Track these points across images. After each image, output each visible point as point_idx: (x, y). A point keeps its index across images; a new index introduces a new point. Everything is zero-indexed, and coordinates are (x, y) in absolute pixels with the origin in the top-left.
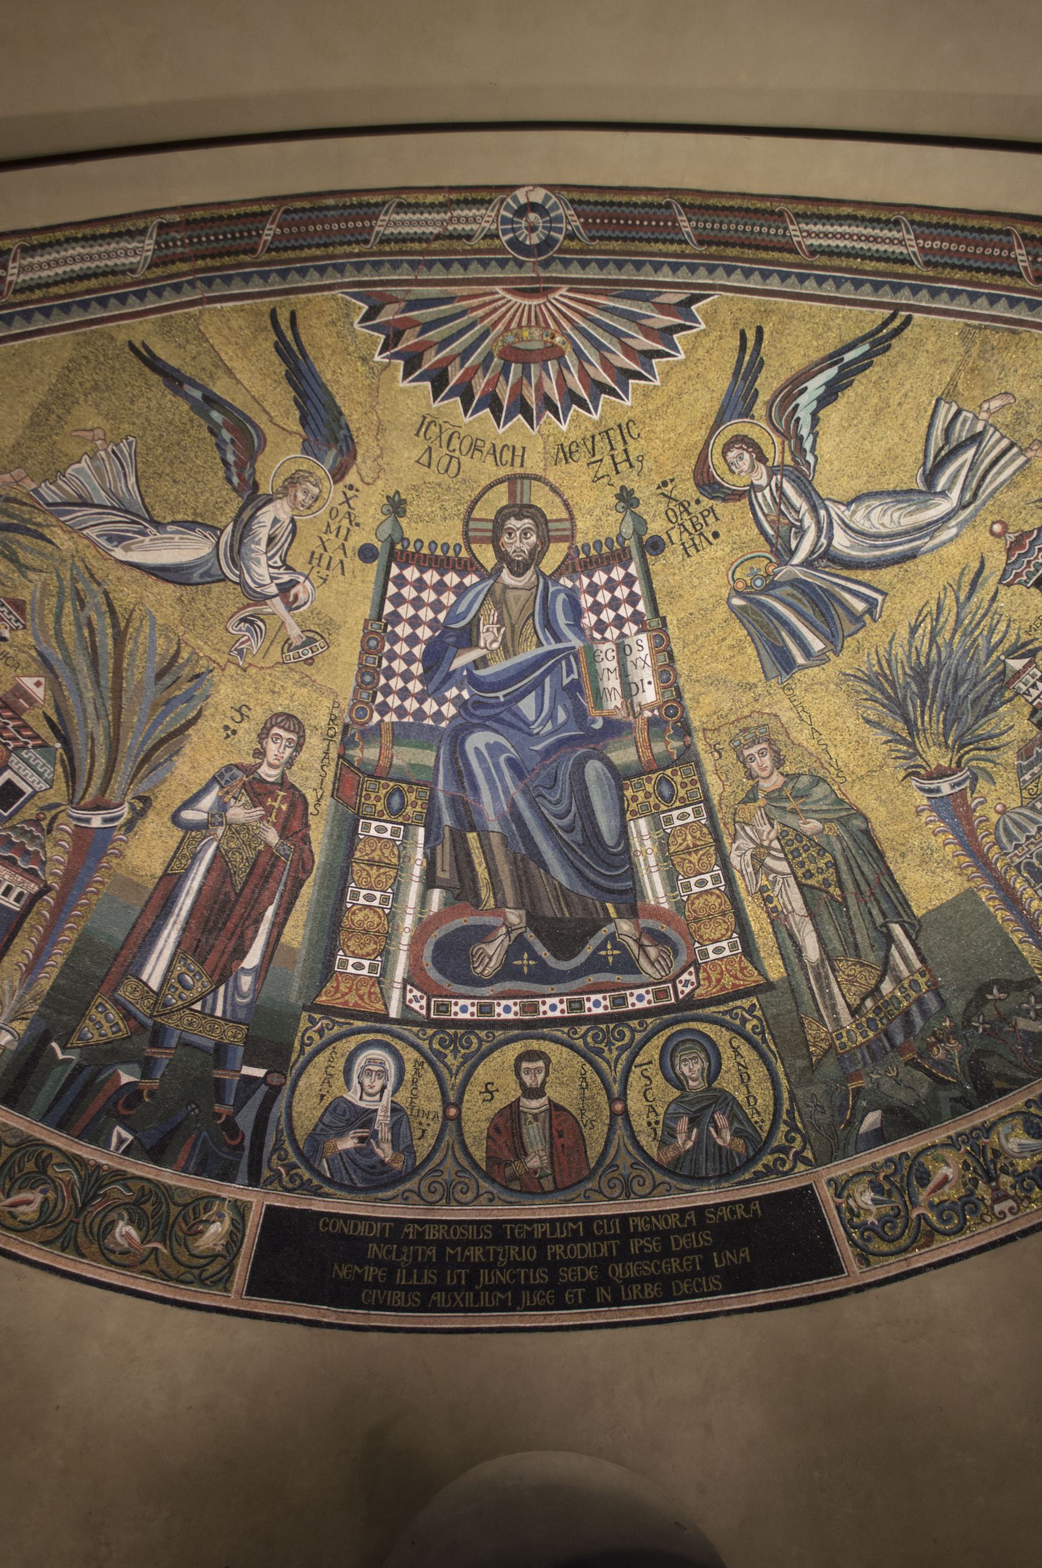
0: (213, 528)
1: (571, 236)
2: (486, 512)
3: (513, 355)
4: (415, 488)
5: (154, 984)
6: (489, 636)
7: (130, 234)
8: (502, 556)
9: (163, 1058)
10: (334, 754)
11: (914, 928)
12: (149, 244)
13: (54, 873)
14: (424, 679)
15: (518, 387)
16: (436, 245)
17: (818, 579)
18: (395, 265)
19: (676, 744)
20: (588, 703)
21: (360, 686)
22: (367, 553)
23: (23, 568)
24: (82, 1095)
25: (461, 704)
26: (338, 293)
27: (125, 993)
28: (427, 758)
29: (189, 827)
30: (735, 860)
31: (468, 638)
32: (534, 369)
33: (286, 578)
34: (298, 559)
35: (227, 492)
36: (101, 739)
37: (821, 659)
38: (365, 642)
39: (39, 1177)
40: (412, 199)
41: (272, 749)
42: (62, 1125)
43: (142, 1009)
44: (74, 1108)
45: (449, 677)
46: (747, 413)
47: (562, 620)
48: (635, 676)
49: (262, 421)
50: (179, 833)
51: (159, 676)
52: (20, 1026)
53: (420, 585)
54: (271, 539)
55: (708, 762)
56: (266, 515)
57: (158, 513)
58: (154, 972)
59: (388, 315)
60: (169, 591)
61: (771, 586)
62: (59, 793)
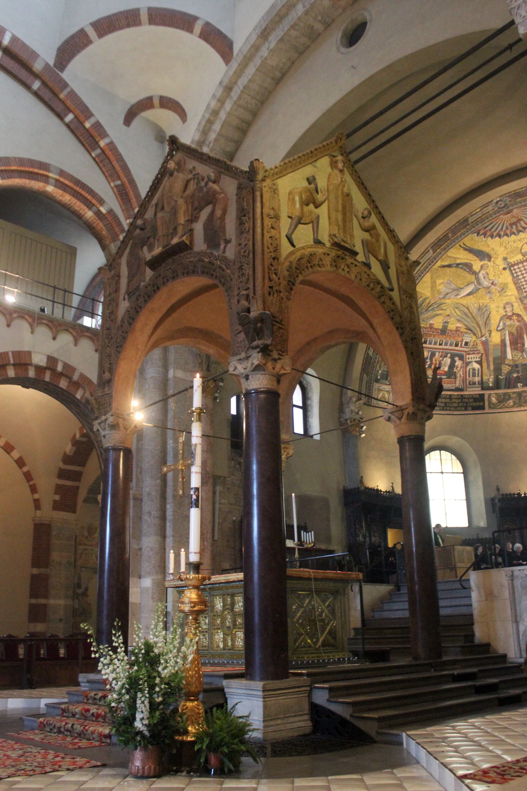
0: (472, 283)
1: (510, 201)
3: (511, 225)
4: (507, 254)
5: (511, 358)
7: (427, 252)
9: (520, 369)
10: (520, 304)
12: (431, 251)
13: (482, 351)
15: (517, 229)
16: (483, 217)
18: (478, 224)
21: (518, 291)
22: (504, 269)
23: (445, 310)
24: (509, 381)
26: (470, 235)
27: (507, 362)
29: (500, 330)
32: (518, 224)
33: (491, 282)
34: (491, 277)
35: (471, 276)
36: (475, 325)
38: (514, 282)
39: (510, 398)
40: (473, 213)
41: (508, 309)
42: (509, 388)
43: (511, 363)
44: (509, 384)
49: (469, 261)
50: (499, 332)
51: (479, 310)
52: (492, 377)
53: (519, 268)
54: (484, 278)
56: (481, 275)
57: (461, 286)
58: (509, 356)
59: (481, 233)
60: (471, 297)
62: (474, 338)
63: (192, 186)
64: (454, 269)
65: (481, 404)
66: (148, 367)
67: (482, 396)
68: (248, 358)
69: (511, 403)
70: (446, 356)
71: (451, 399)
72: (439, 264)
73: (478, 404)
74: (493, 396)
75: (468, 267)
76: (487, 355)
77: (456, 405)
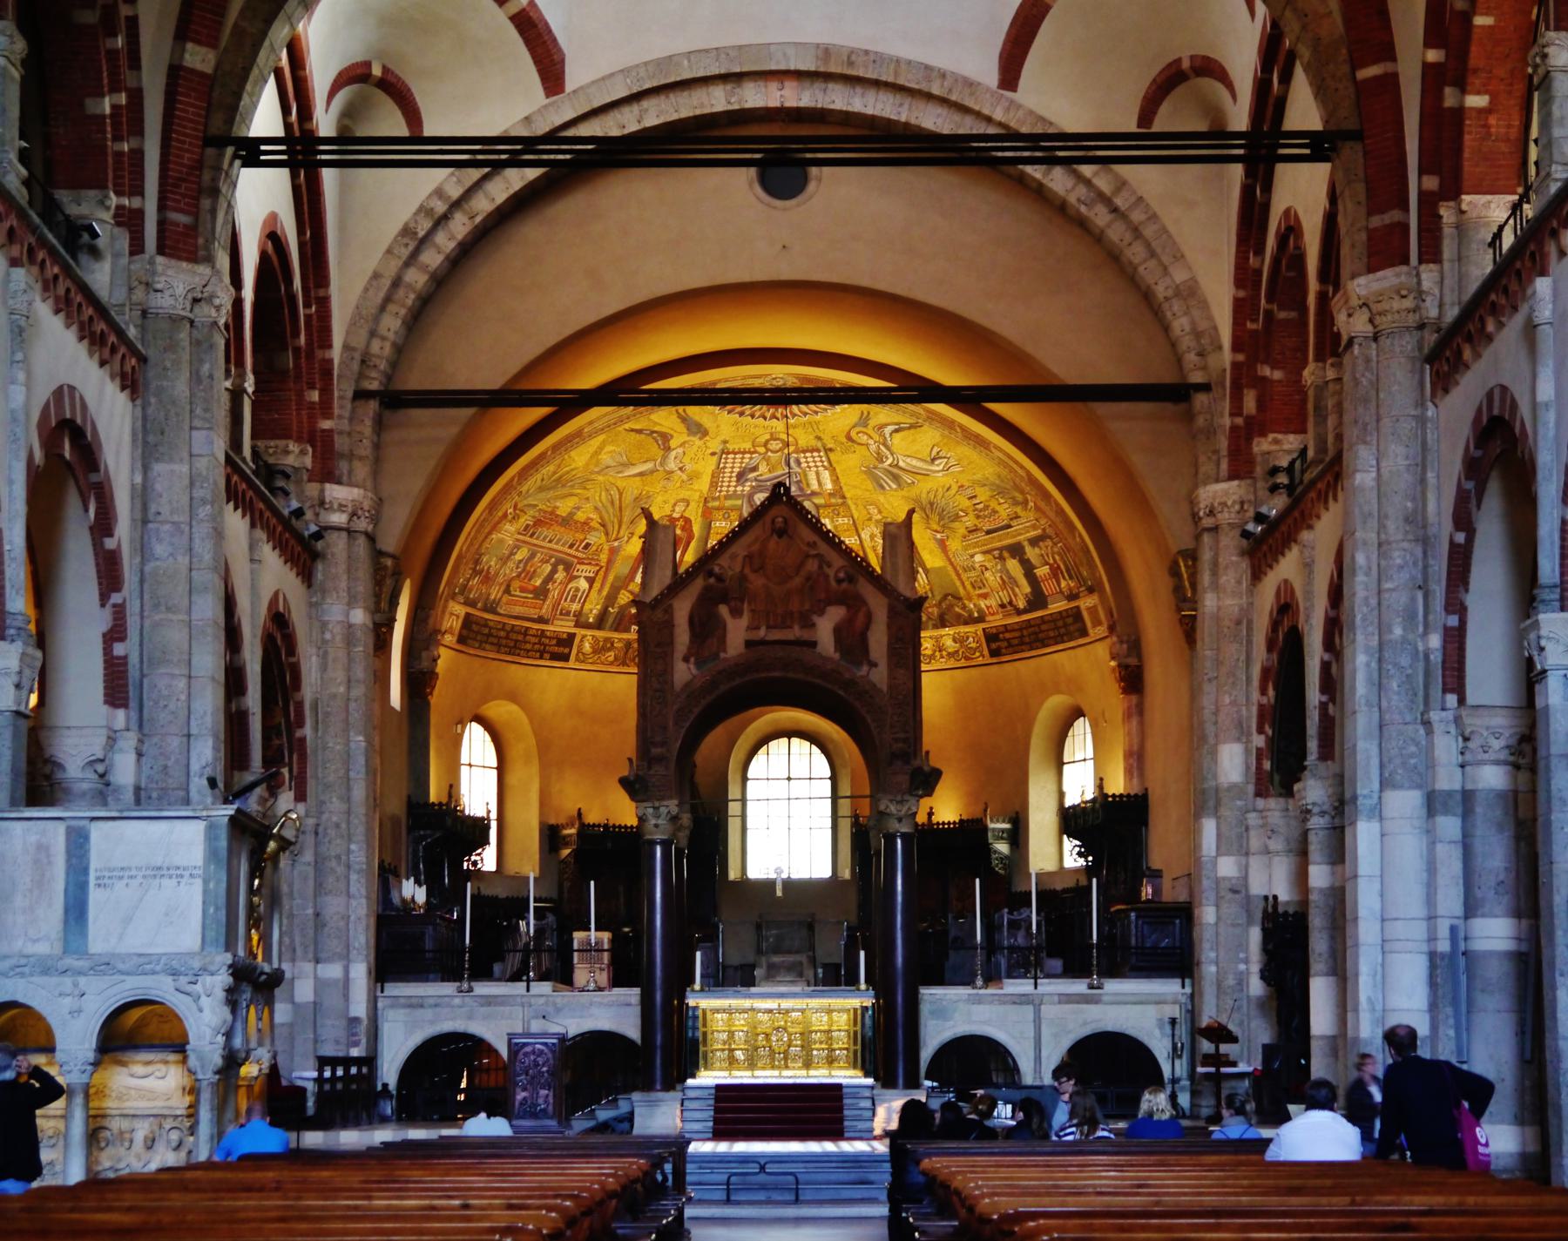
2: (763, 439)
6: (763, 468)
8: (768, 450)
11: (926, 571)
14: (738, 481)
17: (895, 471)
19: (840, 501)
20: (805, 486)
22: (713, 454)
25: (752, 487)
27: (630, 587)
28: (739, 502)
30: (863, 536)
31: (755, 469)
34: (686, 460)
37: (896, 490)
41: (677, 509)
42: (616, 630)
45: (747, 480)
46: (866, 426)
47: (792, 464)
48: (823, 481)
52: (599, 607)
55: (853, 507)
56: (673, 454)
60: (638, 478)
61: (875, 468)
63: (812, 566)
64: (643, 436)
65: (567, 651)
66: (329, 601)
67: (572, 636)
68: (901, 802)
69: (611, 655)
70: (547, 562)
71: (525, 634)
72: (627, 426)
73: (561, 649)
74: (587, 640)
75: (666, 438)
76: (608, 570)
77: (528, 646)
